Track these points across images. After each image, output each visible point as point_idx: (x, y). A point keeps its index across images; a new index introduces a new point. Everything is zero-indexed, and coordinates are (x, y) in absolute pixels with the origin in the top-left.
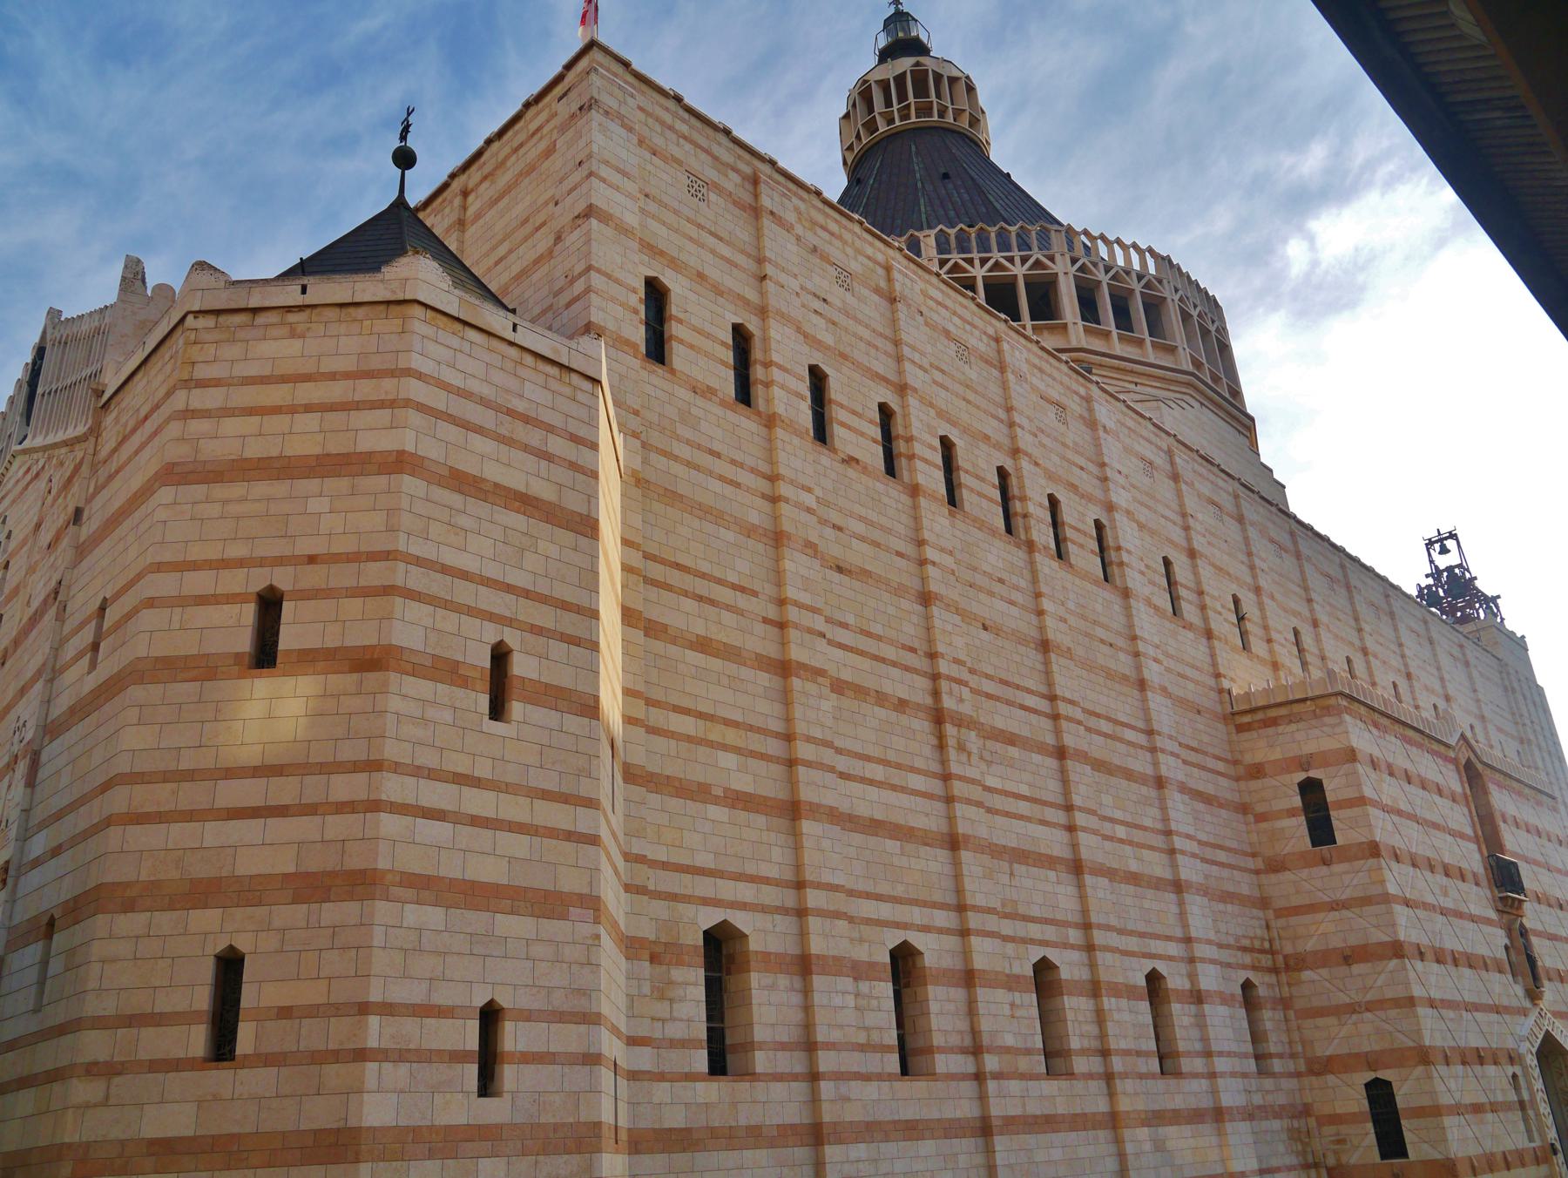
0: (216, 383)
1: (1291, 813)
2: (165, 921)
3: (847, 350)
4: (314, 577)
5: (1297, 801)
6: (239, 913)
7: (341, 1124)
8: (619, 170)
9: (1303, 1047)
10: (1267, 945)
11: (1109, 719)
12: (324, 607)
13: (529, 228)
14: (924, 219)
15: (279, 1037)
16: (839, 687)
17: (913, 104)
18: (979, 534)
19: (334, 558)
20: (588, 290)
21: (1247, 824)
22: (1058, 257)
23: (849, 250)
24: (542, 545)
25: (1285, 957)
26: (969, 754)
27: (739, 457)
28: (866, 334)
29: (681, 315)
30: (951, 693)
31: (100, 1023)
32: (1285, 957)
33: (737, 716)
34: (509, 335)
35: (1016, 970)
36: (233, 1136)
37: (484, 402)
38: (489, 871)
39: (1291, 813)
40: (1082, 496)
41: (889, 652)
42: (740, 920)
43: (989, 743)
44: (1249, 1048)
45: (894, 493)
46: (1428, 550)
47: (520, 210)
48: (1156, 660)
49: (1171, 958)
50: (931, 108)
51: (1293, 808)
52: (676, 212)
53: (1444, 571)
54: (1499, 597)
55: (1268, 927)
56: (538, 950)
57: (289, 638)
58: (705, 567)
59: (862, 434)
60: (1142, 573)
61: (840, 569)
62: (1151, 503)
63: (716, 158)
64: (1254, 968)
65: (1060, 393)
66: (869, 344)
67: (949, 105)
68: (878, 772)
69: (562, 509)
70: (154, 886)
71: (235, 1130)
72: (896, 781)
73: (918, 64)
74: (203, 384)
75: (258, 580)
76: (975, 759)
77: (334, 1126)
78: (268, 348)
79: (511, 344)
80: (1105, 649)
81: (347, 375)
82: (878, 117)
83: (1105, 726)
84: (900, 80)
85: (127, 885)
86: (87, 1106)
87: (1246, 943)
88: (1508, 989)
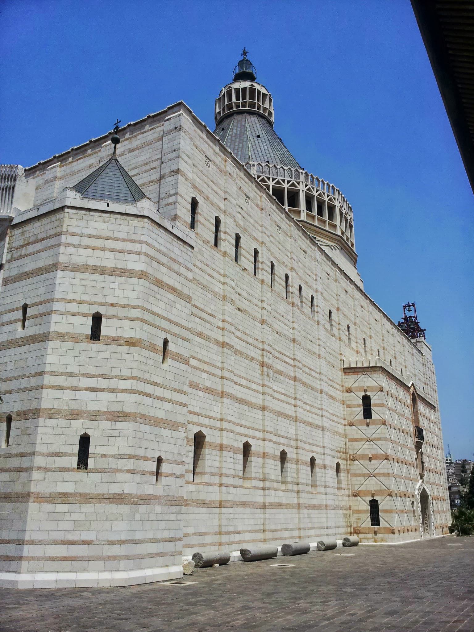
0: (77, 235)
1: (358, 406)
2: (63, 423)
3: (247, 228)
4: (112, 311)
5: (361, 402)
6: (88, 422)
7: (122, 492)
8: (187, 156)
9: (351, 486)
10: (344, 451)
11: (309, 368)
12: (117, 322)
13: (148, 167)
14: (250, 155)
15: (103, 464)
16: (237, 352)
17: (248, 102)
18: (279, 299)
19: (120, 306)
20: (176, 202)
21: (344, 408)
22: (301, 183)
23: (250, 189)
24: (178, 306)
25: (350, 455)
26: (270, 377)
27: (214, 267)
28: (252, 221)
29: (201, 213)
30: (266, 356)
31: (42, 455)
32: (350, 455)
33: (208, 360)
34: (171, 230)
35: (276, 454)
36: (87, 494)
37: (164, 254)
38: (161, 414)
39: (358, 406)
40: (308, 286)
41: (250, 340)
42: (205, 431)
43: (275, 374)
44: (336, 485)
45: (256, 282)
46: (404, 309)
47: (143, 158)
48: (325, 349)
49: (318, 453)
50: (255, 105)
51: (359, 405)
52: (202, 172)
53: (408, 317)
54: (425, 330)
55: (346, 445)
56: (172, 441)
57: (104, 331)
58: (202, 307)
59: (248, 259)
60: (323, 316)
61: (239, 309)
62: (327, 289)
63: (214, 151)
64: (340, 458)
65: (306, 247)
66: (253, 226)
67: (262, 105)
68: (243, 382)
69: (182, 292)
70: (59, 411)
71: (88, 492)
72: (249, 386)
73: (252, 85)
74: (71, 234)
75: (94, 310)
76: (271, 379)
77: (120, 493)
78: (92, 224)
79: (171, 233)
80: (310, 342)
81: (124, 240)
82: (233, 104)
83: (307, 370)
84: (244, 89)
85: (50, 409)
86: (38, 481)
87: (339, 449)
88: (415, 472)
